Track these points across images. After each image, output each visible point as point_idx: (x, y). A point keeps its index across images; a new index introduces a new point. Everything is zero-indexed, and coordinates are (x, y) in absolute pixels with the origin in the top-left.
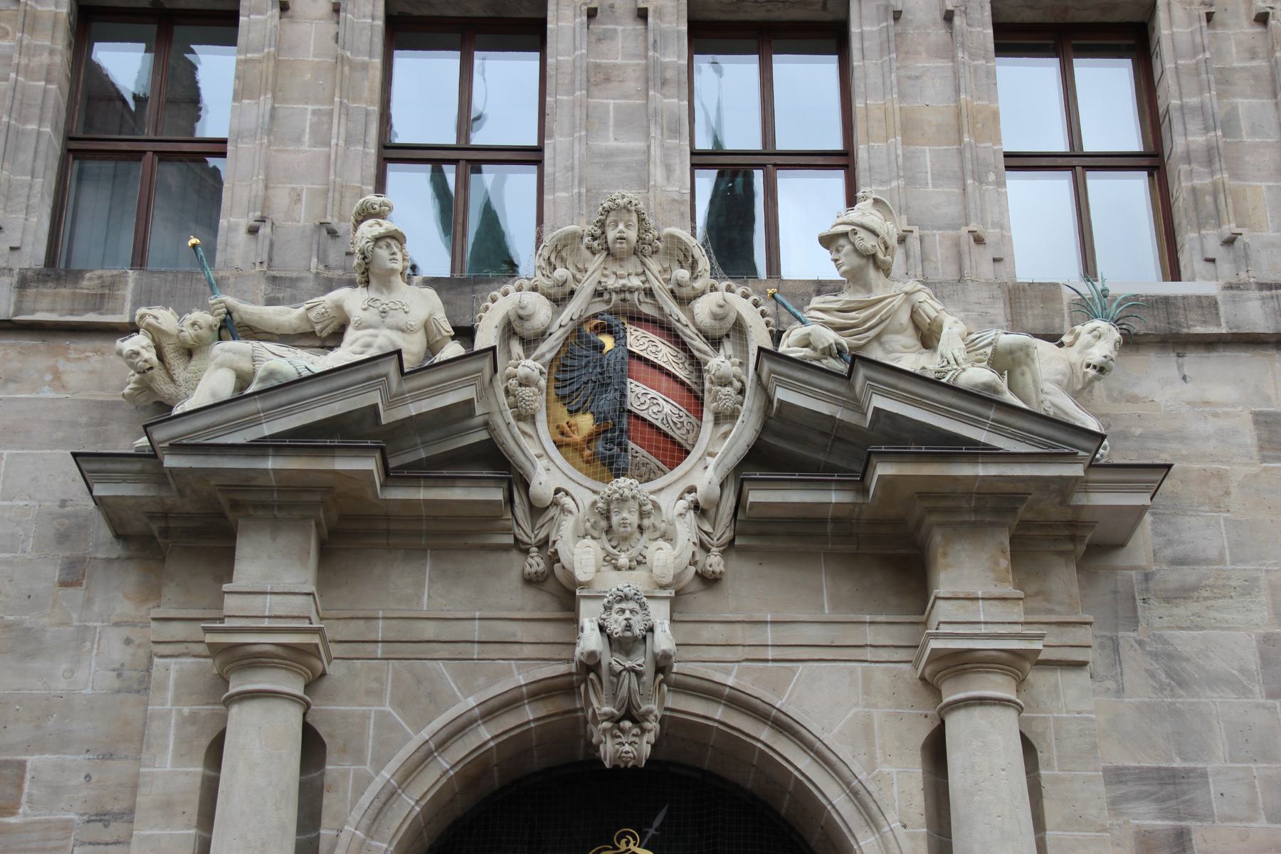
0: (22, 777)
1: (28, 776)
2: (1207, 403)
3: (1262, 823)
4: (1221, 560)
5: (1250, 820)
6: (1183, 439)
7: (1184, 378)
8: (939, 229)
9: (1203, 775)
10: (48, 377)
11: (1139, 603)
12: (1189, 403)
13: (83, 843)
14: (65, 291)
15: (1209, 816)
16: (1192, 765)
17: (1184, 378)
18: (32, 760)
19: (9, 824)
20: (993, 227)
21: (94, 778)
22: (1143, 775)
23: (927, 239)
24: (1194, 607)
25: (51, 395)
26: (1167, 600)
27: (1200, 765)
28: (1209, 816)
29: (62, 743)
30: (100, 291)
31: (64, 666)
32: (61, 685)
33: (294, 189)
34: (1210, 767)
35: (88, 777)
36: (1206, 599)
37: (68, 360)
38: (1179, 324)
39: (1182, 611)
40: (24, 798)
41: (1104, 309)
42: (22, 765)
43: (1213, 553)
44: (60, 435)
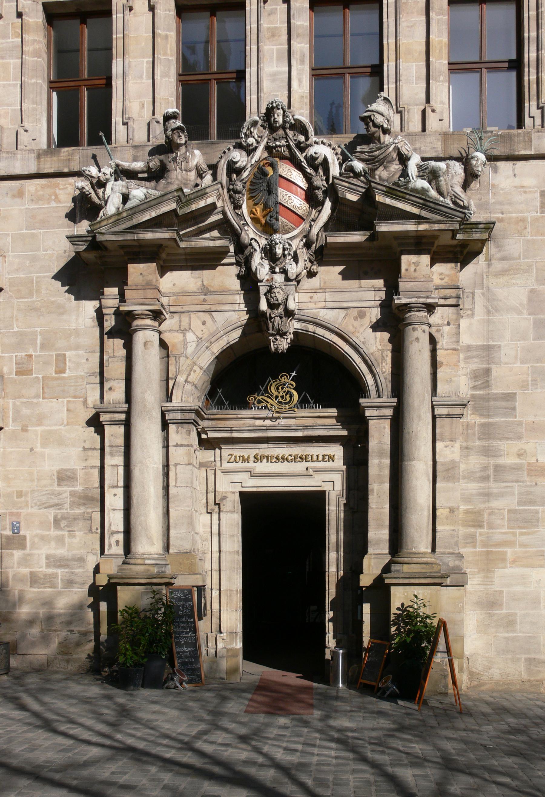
0: (65, 360)
1: (67, 359)
2: (522, 187)
3: (518, 364)
4: (519, 258)
5: (514, 363)
6: (511, 204)
7: (515, 175)
8: (417, 105)
9: (500, 347)
10: (53, 197)
11: (485, 277)
12: (515, 187)
13: (89, 384)
14: (55, 159)
15: (500, 363)
16: (496, 343)
17: (515, 175)
18: (68, 353)
19: (64, 377)
20: (440, 104)
21: (90, 360)
22: (478, 348)
23: (411, 111)
24: (506, 278)
25: (55, 205)
26: (496, 276)
27: (499, 343)
28: (500, 363)
29: (77, 347)
30: (68, 158)
31: (74, 317)
32: (74, 326)
33: (141, 102)
34: (503, 344)
35: (87, 359)
36: (511, 275)
37: (60, 189)
38: (514, 150)
39: (502, 280)
40: (67, 367)
41: (481, 146)
42: (65, 355)
43: (516, 255)
44: (60, 222)
